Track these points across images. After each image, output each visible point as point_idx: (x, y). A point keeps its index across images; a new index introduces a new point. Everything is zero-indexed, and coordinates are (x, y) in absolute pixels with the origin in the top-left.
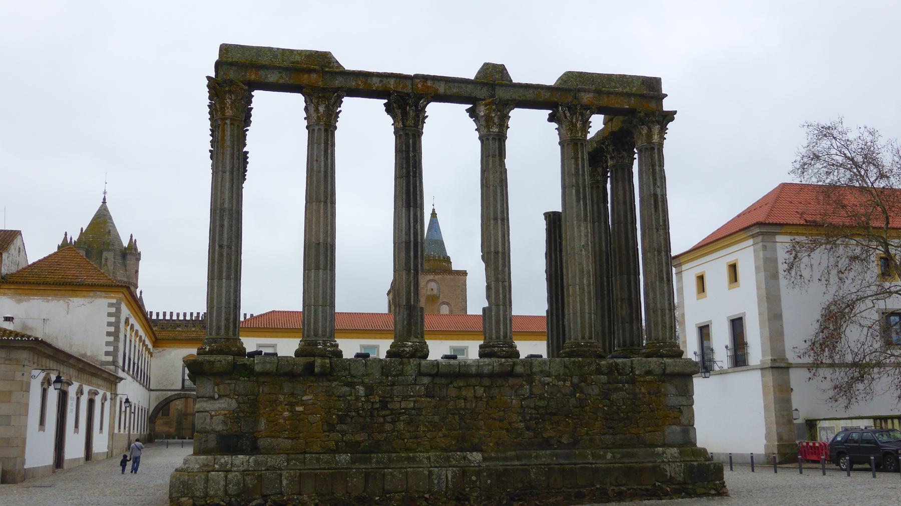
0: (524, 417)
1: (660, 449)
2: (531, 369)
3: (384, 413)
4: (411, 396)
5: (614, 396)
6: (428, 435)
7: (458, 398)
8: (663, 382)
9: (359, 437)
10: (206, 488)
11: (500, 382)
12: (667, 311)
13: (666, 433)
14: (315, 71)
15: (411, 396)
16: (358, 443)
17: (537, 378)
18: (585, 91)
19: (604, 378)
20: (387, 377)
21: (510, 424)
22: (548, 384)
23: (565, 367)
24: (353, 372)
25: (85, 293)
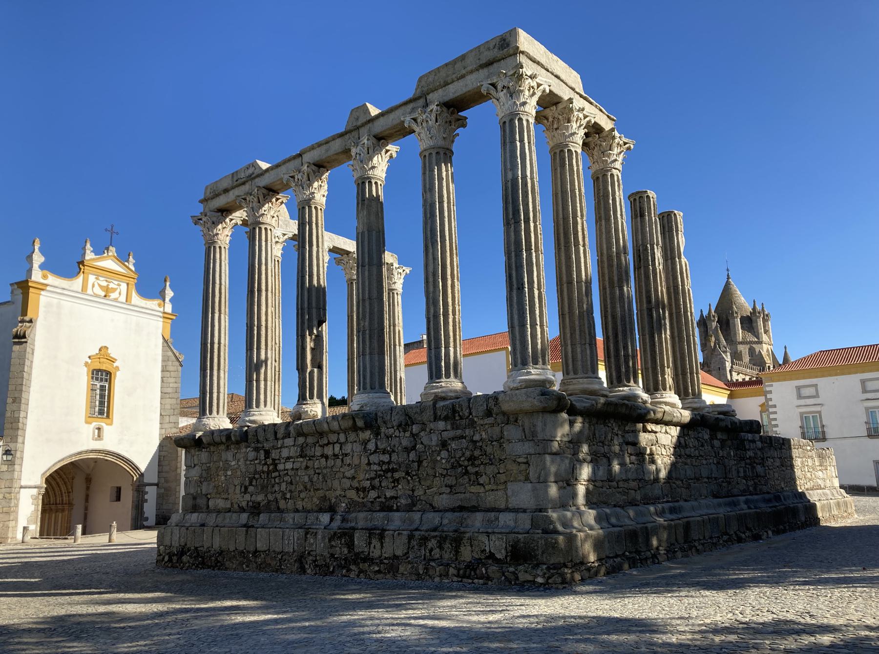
1: (493, 514)
2: (376, 420)
3: (274, 475)
5: (454, 445)
6: (303, 495)
9: (260, 498)
11: (352, 436)
12: (517, 328)
13: (509, 492)
15: (292, 457)
16: (259, 503)
17: (383, 430)
19: (441, 425)
21: (359, 482)
23: (407, 415)
24: (261, 439)
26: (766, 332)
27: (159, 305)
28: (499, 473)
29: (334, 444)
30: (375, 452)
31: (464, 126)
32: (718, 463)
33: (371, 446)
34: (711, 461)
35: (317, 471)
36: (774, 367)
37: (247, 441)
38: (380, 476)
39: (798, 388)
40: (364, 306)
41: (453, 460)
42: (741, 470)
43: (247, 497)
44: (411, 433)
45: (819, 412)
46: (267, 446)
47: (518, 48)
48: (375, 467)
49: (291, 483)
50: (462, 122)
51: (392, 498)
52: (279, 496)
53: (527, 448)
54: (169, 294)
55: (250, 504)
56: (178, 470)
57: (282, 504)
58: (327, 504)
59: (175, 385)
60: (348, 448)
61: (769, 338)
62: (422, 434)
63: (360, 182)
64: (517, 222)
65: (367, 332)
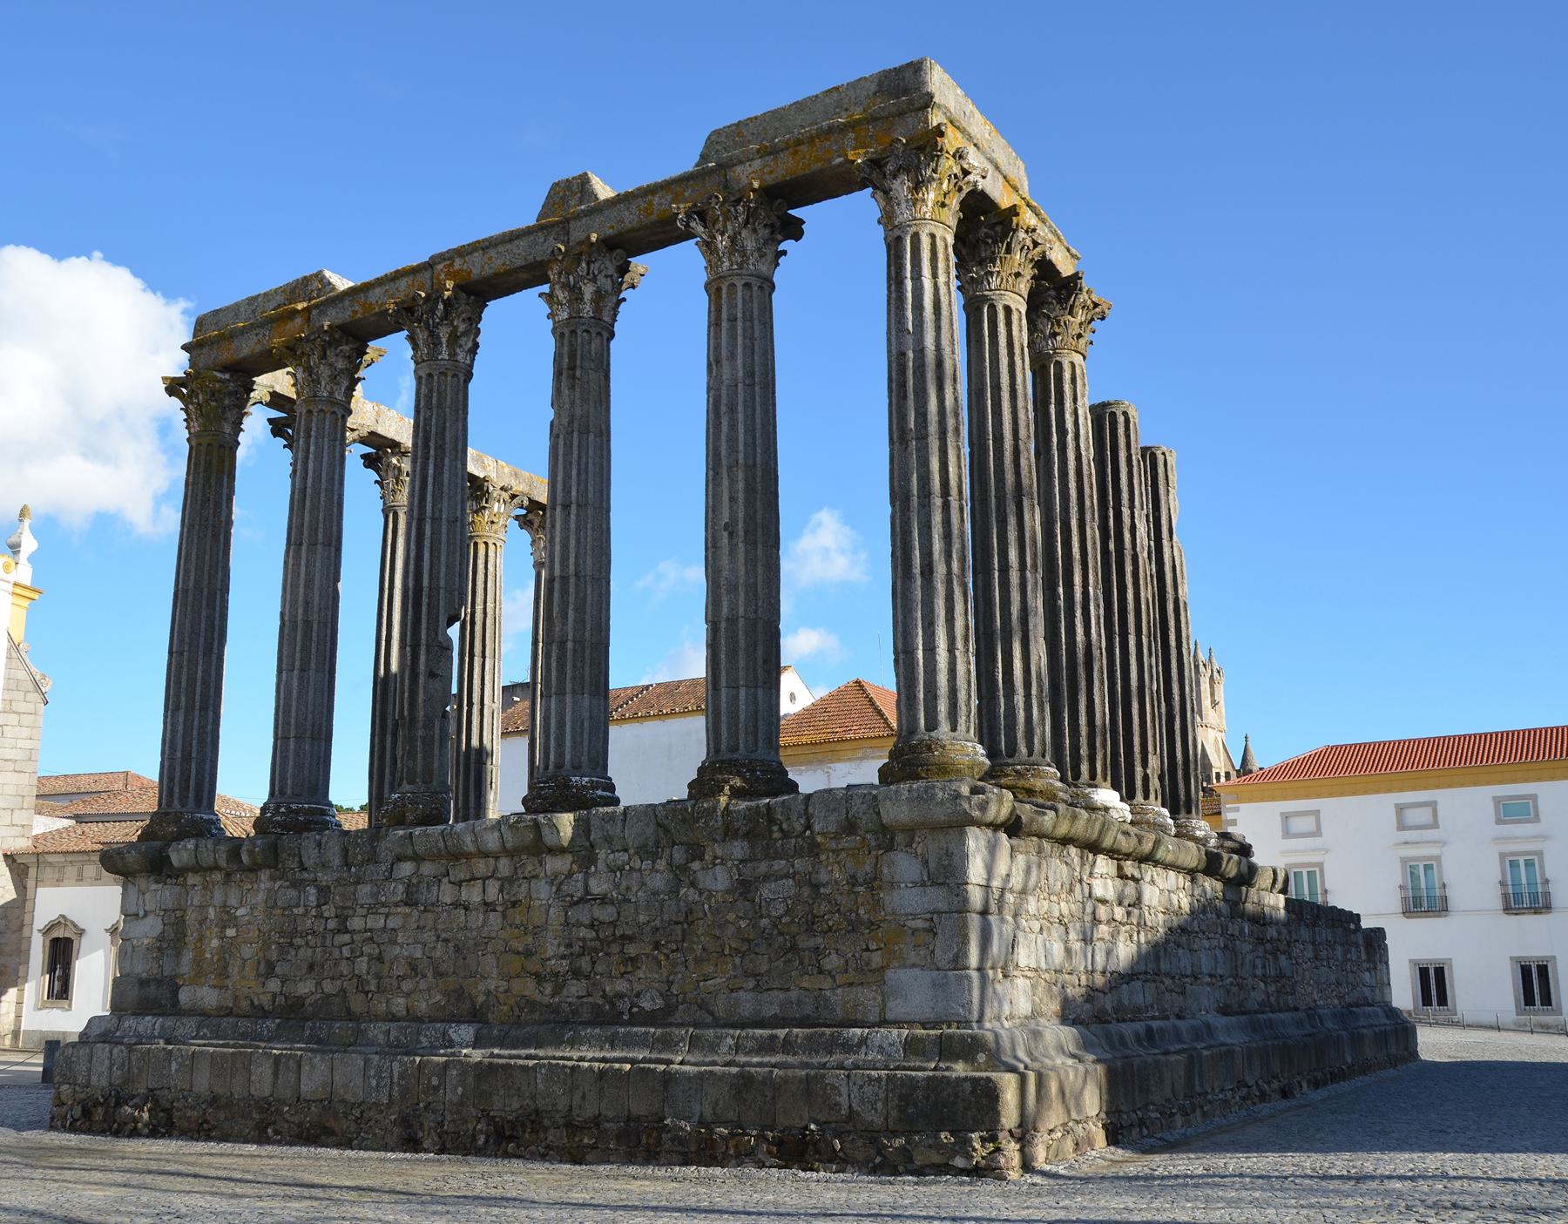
0: (569, 946)
2: (588, 832)
4: (384, 905)
5: (766, 891)
6: (407, 986)
7: (456, 905)
8: (890, 847)
9: (304, 988)
10: (89, 1069)
11: (530, 866)
14: (296, 311)
17: (602, 854)
18: (741, 162)
19: (738, 849)
20: (348, 865)
22: (621, 869)
23: (658, 824)
25: (849, 754)
26: (1214, 704)
27: (6, 568)
28: (867, 949)
29: (484, 879)
30: (582, 900)
31: (798, 235)
32: (1226, 947)
33: (575, 888)
34: (1215, 943)
35: (444, 935)
36: (1228, 775)
37: (275, 867)
38: (596, 950)
39: (1286, 817)
40: (565, 592)
41: (764, 922)
42: (1259, 962)
43: (274, 985)
44: (670, 864)
45: (1321, 865)
46: (325, 878)
47: (931, 96)
48: (584, 933)
49: (380, 959)
50: (794, 230)
51: (621, 996)
52: (350, 987)
53: (936, 898)
54: (29, 544)
55: (280, 1000)
56: (26, 932)
57: (357, 1003)
58: (467, 1005)
59: (28, 744)
60: (521, 891)
61: (1220, 717)
62: (696, 865)
63: (566, 331)
64: (923, 437)
65: (570, 645)
